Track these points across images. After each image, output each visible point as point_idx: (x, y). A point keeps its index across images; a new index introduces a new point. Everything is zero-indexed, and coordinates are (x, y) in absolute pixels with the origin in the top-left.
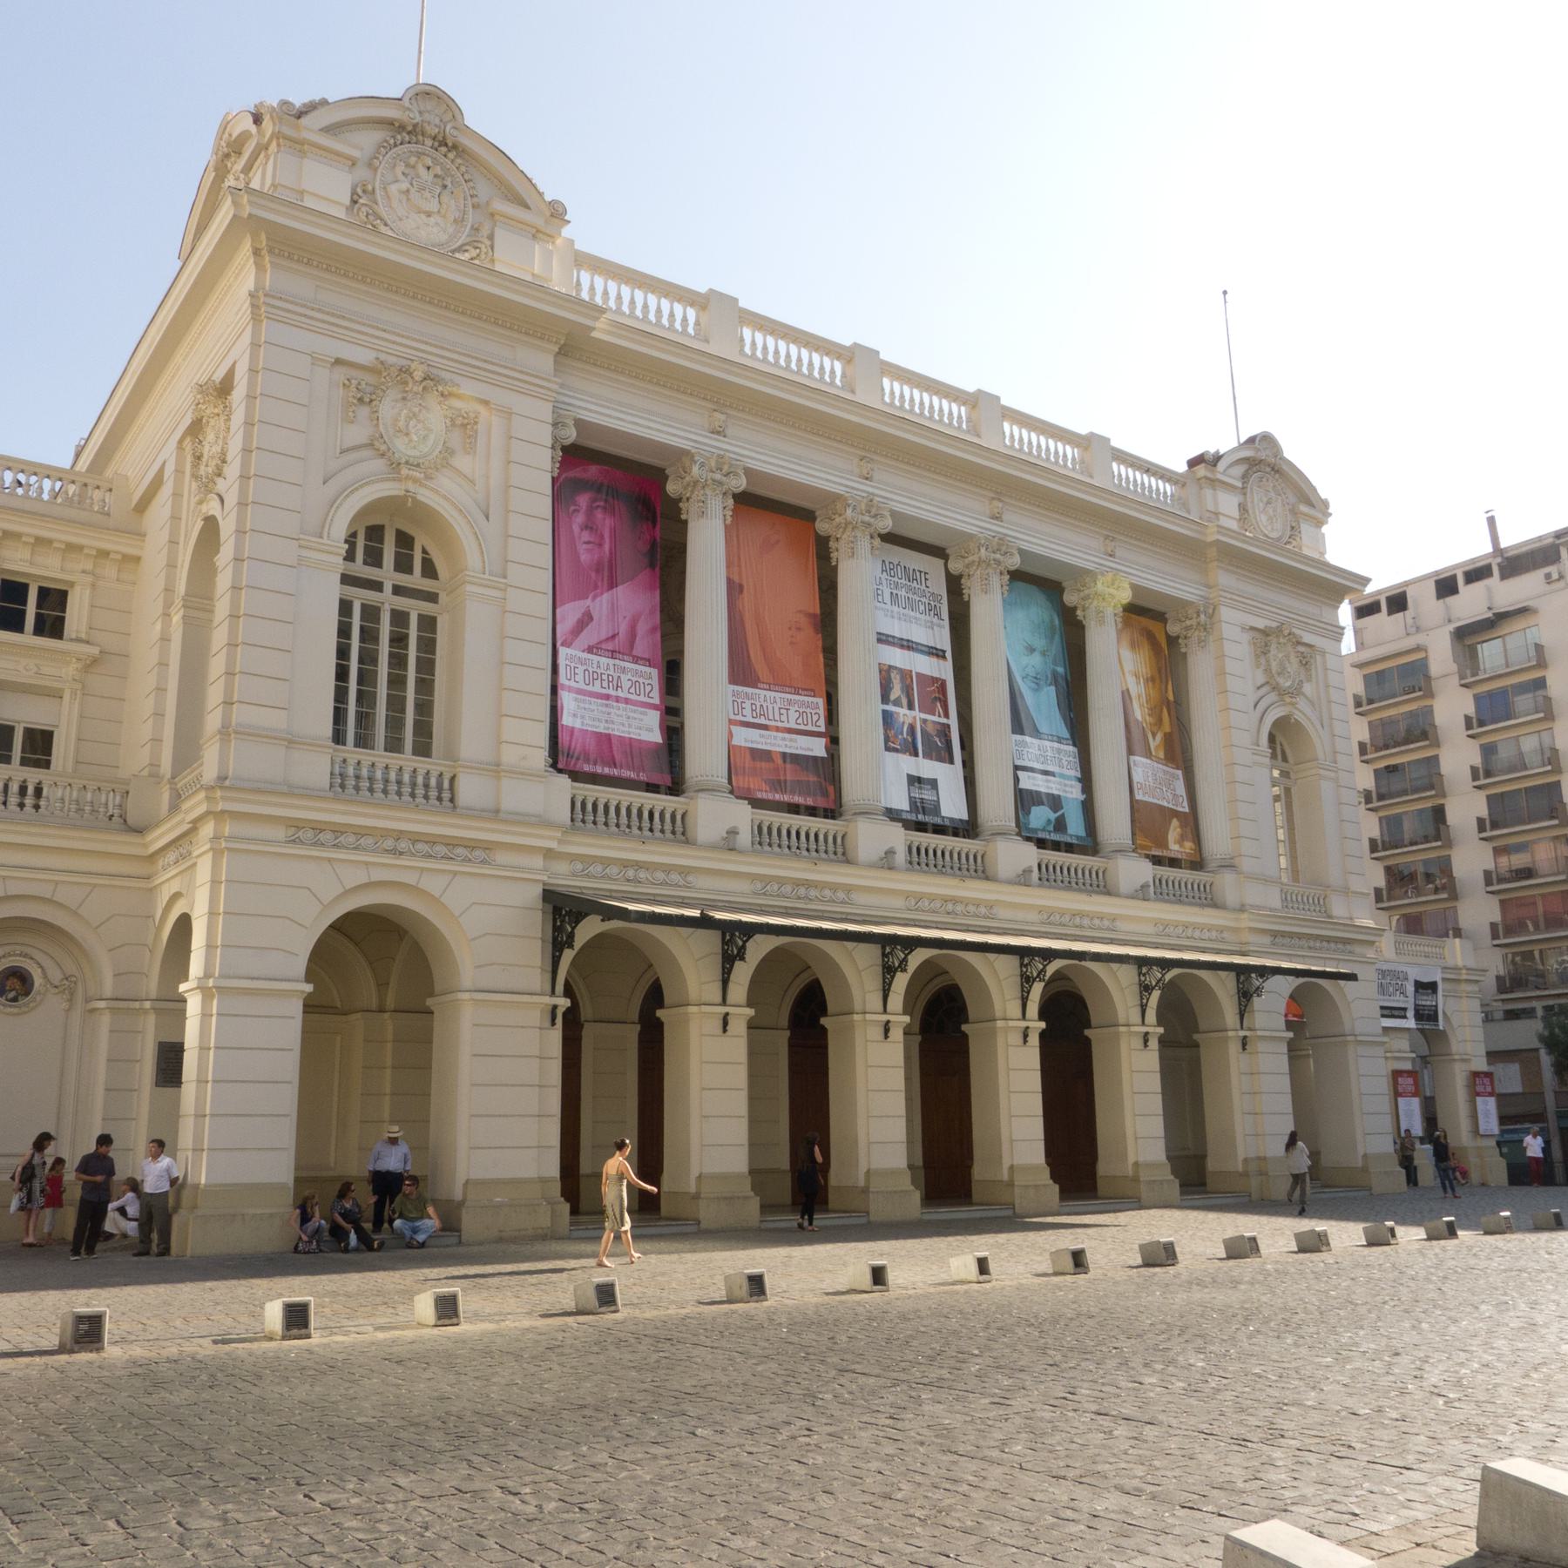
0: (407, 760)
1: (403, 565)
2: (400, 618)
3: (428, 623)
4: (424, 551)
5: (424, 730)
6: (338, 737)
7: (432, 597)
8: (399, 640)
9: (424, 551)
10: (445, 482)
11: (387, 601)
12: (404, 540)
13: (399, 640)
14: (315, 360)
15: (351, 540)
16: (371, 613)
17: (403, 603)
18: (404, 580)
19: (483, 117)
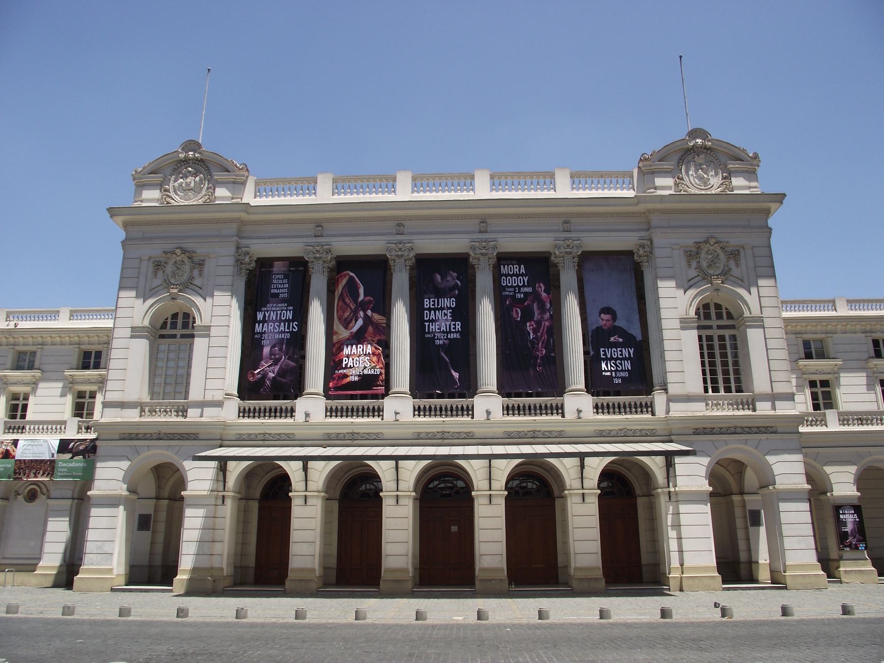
1: (719, 316)
2: (722, 338)
3: (734, 338)
7: (733, 327)
8: (723, 347)
13: (723, 347)
17: (721, 332)
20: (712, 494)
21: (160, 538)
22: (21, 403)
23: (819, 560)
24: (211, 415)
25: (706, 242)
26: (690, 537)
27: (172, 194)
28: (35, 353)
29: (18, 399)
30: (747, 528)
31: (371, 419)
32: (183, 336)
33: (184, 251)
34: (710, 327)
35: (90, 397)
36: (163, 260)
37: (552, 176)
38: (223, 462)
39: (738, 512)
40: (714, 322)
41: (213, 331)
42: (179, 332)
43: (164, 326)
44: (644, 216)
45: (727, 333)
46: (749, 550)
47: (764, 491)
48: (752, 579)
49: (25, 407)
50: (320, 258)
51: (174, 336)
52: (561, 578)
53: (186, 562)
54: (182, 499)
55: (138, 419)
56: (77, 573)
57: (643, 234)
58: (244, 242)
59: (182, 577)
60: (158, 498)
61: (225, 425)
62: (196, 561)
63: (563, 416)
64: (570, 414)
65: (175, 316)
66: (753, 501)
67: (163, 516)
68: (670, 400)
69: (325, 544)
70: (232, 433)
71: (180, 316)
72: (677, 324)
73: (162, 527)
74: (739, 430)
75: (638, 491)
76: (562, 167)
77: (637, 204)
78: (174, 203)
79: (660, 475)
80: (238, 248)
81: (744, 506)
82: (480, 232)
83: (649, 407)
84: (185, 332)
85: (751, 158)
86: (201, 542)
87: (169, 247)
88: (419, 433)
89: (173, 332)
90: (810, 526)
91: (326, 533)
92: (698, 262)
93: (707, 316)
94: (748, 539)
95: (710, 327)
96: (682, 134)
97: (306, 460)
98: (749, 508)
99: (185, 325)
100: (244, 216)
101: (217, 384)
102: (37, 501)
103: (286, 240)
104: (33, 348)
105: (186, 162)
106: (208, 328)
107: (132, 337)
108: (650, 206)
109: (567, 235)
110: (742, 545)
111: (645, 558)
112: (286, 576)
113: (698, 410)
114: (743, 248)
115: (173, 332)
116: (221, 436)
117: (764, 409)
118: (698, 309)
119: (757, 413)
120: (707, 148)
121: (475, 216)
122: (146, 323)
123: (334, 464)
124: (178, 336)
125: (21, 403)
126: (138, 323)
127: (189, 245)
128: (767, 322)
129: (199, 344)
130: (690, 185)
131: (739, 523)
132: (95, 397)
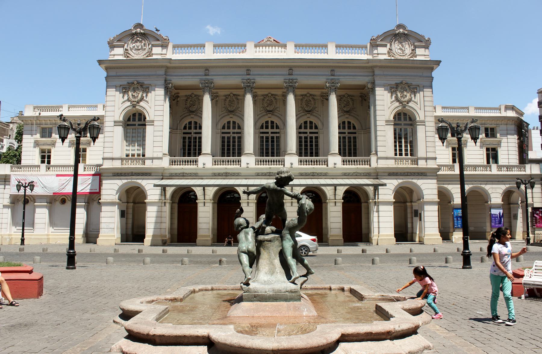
1: (405, 119)
10: (410, 104)
15: (394, 118)
19: (411, 27)
20: (394, 202)
21: (130, 221)
22: (46, 154)
23: (440, 232)
24: (157, 164)
25: (401, 83)
26: (382, 222)
27: (130, 52)
28: (51, 128)
29: (45, 152)
30: (412, 218)
31: (235, 166)
32: (139, 125)
33: (138, 83)
35: (83, 151)
36: (127, 87)
37: (326, 46)
38: (164, 188)
39: (409, 210)
40: (403, 122)
41: (156, 123)
42: (137, 123)
43: (129, 120)
44: (371, 68)
46: (412, 228)
47: (419, 202)
48: (412, 240)
49: (49, 157)
50: (208, 86)
51: (135, 125)
52: (324, 240)
53: (149, 233)
54: (145, 203)
55: (120, 166)
56: (98, 237)
57: (370, 78)
58: (168, 78)
59: (148, 239)
60: (128, 202)
61: (164, 169)
62: (154, 232)
63: (327, 166)
64: (331, 165)
65: (134, 115)
66: (415, 206)
67: (130, 211)
68: (378, 159)
69: (213, 224)
70: (167, 173)
71: (137, 115)
72: (384, 123)
73: (130, 216)
74: (409, 174)
75: (362, 200)
76: (332, 42)
77: (368, 63)
78: (134, 58)
79: (371, 194)
80: (165, 81)
81: (412, 207)
82: (289, 75)
83: (368, 162)
85: (427, 41)
86: (156, 223)
87: (131, 80)
88: (258, 173)
89: (135, 123)
90: (437, 217)
91: (213, 219)
94: (412, 223)
96: (393, 27)
97: (204, 187)
98: (414, 209)
99: (140, 120)
100: (168, 65)
101: (159, 149)
102: (66, 204)
103: (190, 77)
104: (51, 126)
105: (136, 34)
106: (153, 121)
107: (115, 125)
108: (375, 64)
109: (333, 77)
110: (409, 225)
111: (364, 231)
112: (196, 238)
113: (391, 164)
114: (418, 86)
115: (134, 123)
116: (162, 174)
117: (422, 164)
119: (419, 166)
120: (404, 34)
121: (287, 66)
122: (121, 119)
123: (216, 188)
125: (46, 154)
126: (117, 119)
127: (141, 80)
128: (427, 124)
129: (149, 129)
130: (395, 53)
131: (409, 215)
132: (86, 151)
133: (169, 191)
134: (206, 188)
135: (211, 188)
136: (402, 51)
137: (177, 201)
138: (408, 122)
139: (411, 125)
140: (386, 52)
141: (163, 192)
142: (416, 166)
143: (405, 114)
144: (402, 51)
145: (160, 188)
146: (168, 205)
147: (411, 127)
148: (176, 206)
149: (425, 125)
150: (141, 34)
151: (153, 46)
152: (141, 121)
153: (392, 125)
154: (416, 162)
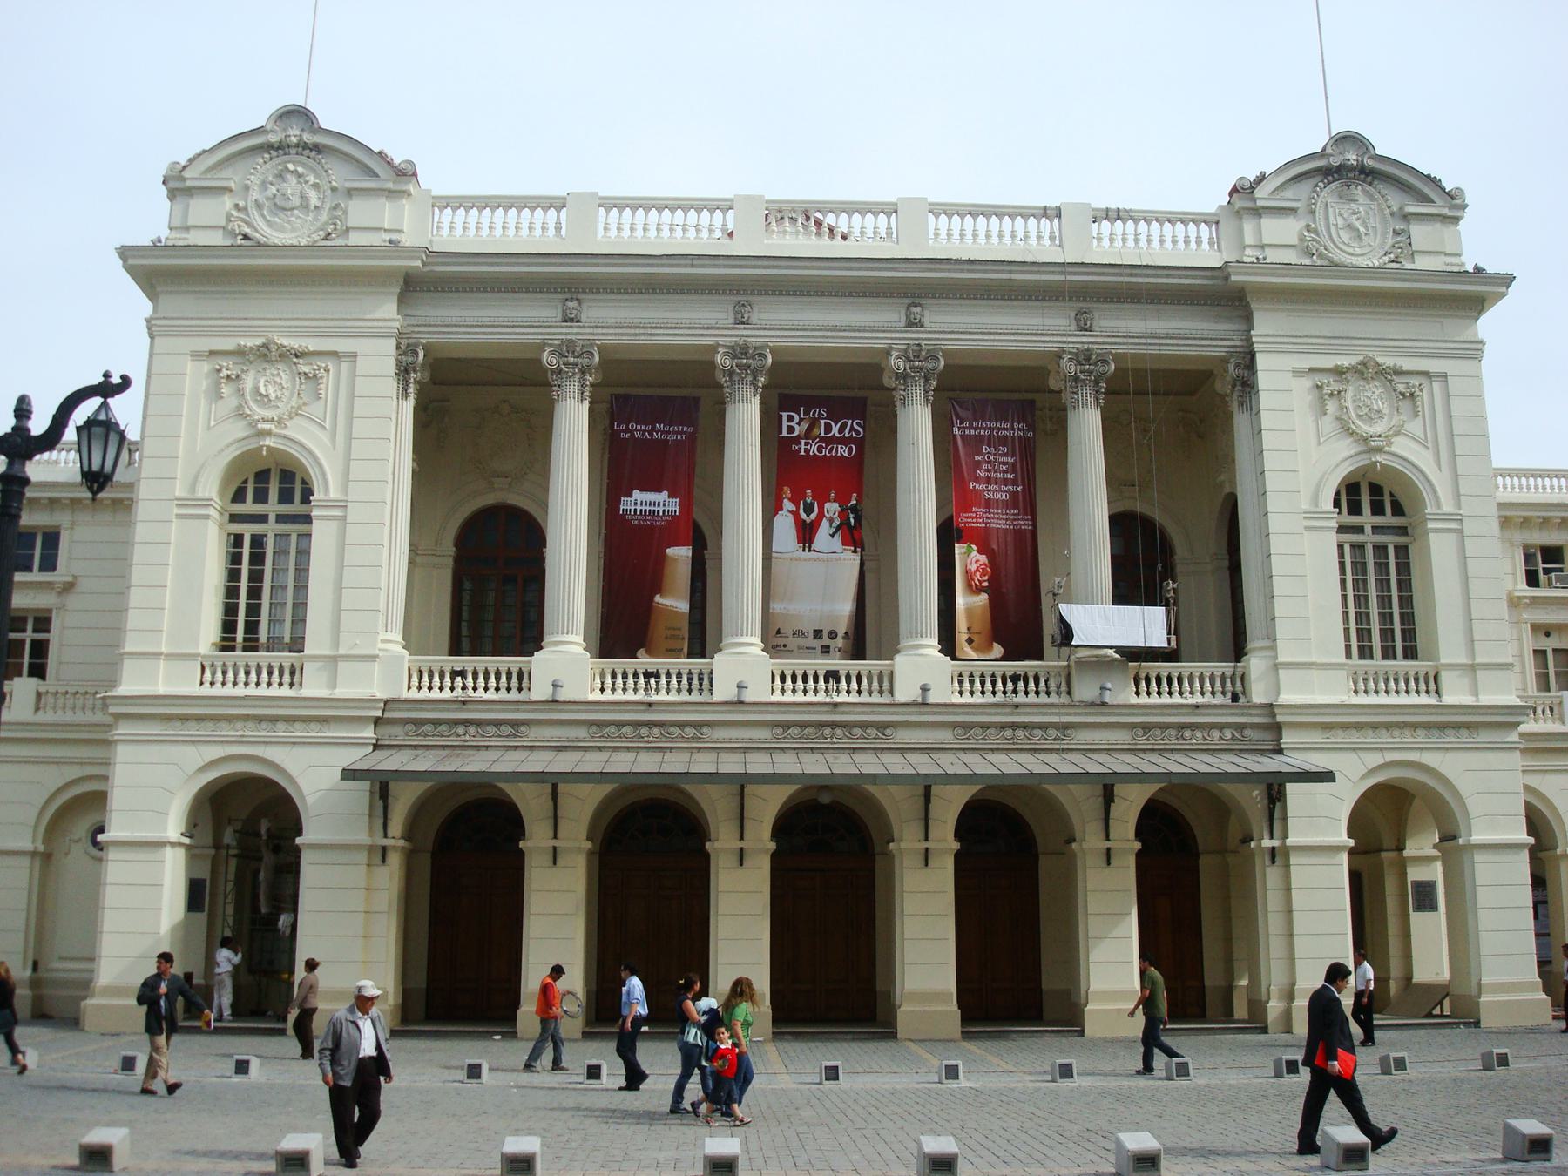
0: (1400, 664)
1: (1377, 509)
2: (1380, 550)
3: (1402, 551)
4: (1392, 495)
5: (1409, 634)
6: (1349, 655)
9: (1392, 495)
11: (1369, 538)
12: (1376, 490)
14: (1297, 372)
15: (1337, 504)
16: (1358, 548)
18: (1379, 520)
19: (1388, 144)
34: (1359, 530)
40: (1367, 519)
45: (1390, 541)
65: (262, 476)
84: (286, 509)
92: (1342, 408)
93: (1355, 509)
95: (1359, 530)
99: (286, 497)
118: (1338, 493)
124: (272, 518)
133: (404, 800)
134: (561, 787)
135: (584, 789)
136: (1356, 236)
137: (429, 845)
138: (1388, 519)
139: (1403, 531)
140: (1295, 241)
141: (380, 804)
142: (1432, 700)
143: (1376, 490)
144: (1356, 236)
145: (366, 785)
146: (395, 860)
147: (1401, 540)
148: (425, 862)
149: (1461, 531)
150: (303, 146)
151: (350, 193)
152: (291, 501)
153: (1328, 529)
154: (1433, 682)
